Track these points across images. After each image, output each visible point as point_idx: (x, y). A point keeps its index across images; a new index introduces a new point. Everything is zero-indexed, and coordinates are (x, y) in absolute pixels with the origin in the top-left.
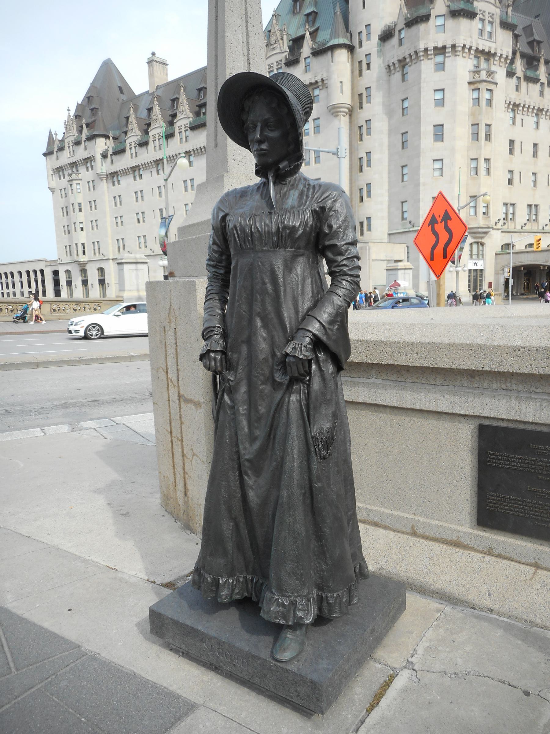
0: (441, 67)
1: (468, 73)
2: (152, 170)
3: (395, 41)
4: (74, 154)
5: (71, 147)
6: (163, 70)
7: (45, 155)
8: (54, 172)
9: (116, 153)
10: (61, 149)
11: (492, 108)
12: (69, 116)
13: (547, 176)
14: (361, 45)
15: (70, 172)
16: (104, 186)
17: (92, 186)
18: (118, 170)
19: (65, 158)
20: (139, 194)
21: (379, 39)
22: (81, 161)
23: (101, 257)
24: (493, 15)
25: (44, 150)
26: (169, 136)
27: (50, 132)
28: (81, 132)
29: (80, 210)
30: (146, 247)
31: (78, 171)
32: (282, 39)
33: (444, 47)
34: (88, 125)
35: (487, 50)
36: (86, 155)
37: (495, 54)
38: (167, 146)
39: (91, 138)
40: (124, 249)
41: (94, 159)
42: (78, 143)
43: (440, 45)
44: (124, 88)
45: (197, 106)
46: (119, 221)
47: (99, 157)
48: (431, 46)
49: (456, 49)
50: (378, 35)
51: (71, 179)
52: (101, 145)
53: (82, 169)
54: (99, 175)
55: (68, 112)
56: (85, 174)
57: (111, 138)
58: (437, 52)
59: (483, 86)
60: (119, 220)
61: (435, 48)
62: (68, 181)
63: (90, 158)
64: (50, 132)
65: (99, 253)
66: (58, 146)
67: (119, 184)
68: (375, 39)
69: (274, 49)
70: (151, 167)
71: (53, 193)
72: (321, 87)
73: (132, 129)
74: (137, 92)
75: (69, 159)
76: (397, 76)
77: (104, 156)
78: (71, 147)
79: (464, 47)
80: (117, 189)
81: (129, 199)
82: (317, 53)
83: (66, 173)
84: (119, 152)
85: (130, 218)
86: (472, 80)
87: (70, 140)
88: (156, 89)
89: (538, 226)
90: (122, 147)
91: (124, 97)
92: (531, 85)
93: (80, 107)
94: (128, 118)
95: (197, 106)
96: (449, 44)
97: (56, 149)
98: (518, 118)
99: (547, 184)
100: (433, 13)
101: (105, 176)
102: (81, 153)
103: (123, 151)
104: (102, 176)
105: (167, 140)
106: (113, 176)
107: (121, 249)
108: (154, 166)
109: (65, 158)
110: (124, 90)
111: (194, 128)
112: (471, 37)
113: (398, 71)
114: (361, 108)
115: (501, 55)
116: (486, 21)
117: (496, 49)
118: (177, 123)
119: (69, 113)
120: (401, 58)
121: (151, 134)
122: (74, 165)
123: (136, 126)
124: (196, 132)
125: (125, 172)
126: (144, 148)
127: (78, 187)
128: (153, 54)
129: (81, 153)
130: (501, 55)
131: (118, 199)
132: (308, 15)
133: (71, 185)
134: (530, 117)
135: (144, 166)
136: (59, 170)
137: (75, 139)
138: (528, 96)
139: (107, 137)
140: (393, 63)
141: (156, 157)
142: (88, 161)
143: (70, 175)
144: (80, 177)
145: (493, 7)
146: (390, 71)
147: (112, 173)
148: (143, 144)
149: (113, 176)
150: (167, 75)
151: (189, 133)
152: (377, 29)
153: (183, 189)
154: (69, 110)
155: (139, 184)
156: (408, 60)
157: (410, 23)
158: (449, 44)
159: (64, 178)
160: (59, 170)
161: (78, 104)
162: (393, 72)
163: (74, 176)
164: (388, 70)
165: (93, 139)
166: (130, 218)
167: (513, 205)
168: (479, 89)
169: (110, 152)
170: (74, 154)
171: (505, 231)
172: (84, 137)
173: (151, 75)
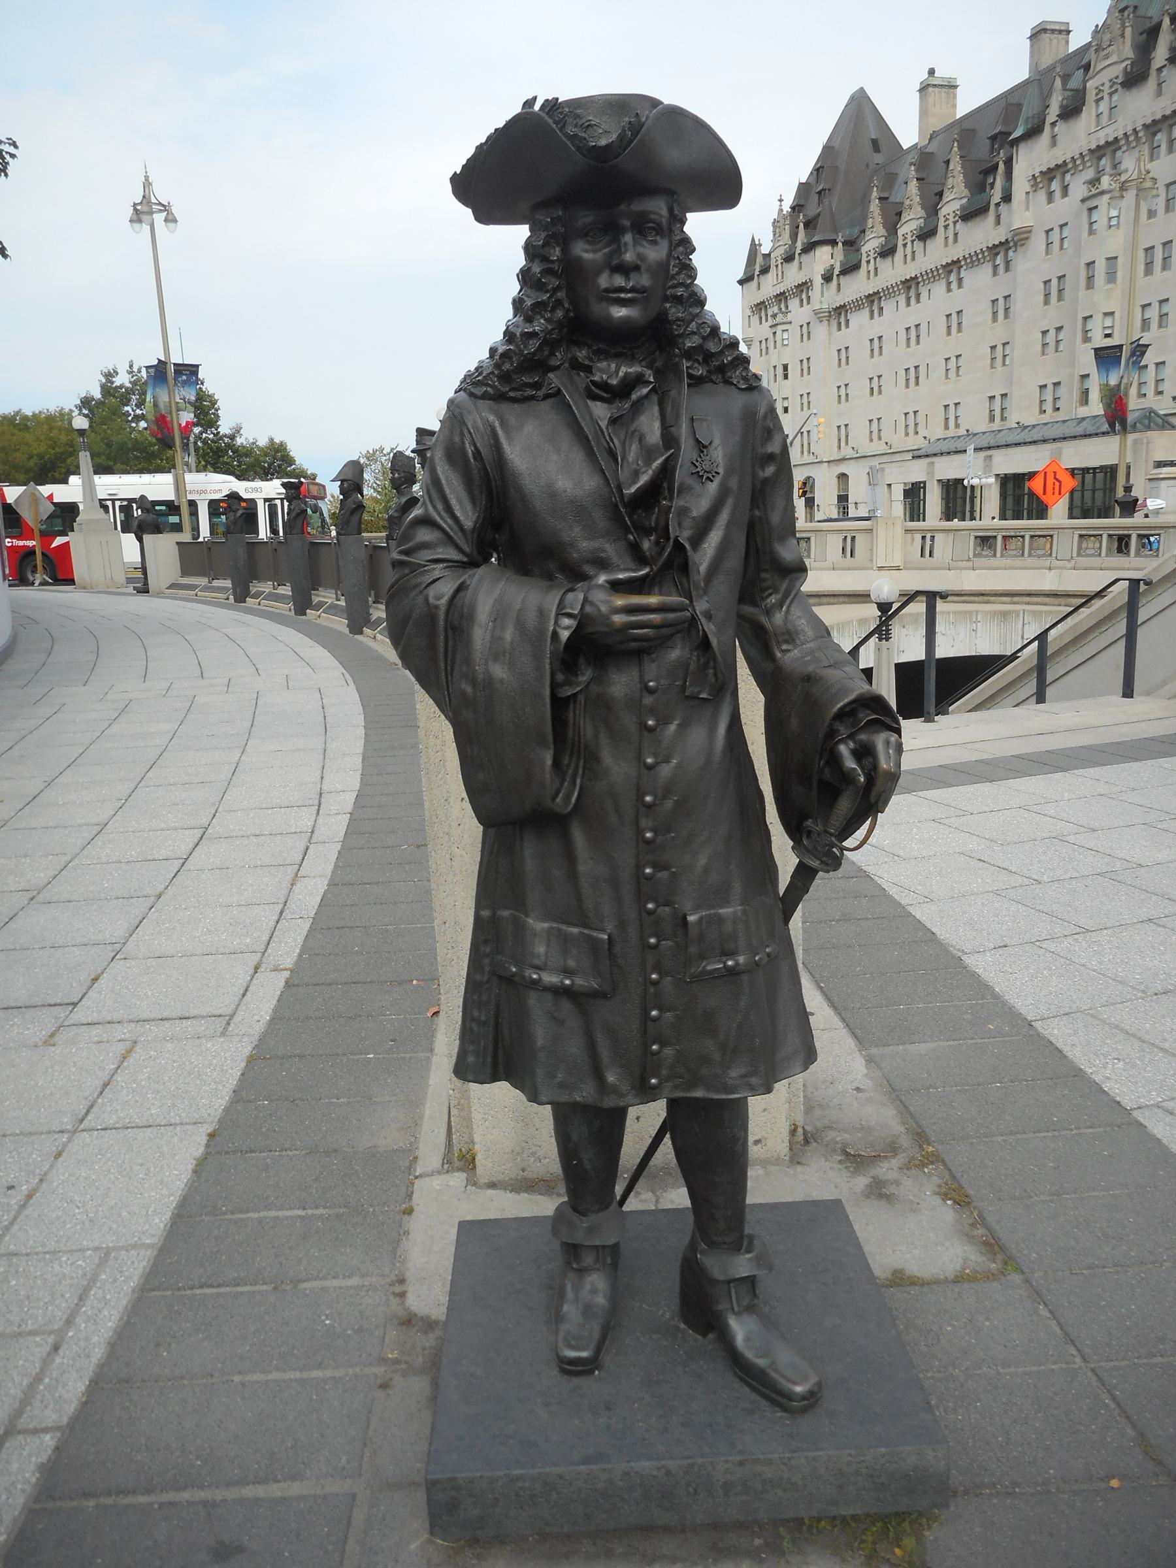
2: (898, 298)
4: (783, 278)
5: (780, 266)
7: (741, 282)
8: (753, 312)
9: (845, 272)
10: (765, 271)
12: (781, 210)
15: (776, 309)
16: (821, 331)
17: (806, 332)
19: (769, 286)
20: (876, 345)
22: (792, 290)
23: (812, 459)
25: (740, 275)
26: (926, 235)
27: (753, 238)
29: (786, 377)
30: (880, 438)
31: (787, 307)
32: (1123, 36)
34: (807, 225)
38: (923, 253)
39: (809, 248)
40: (847, 443)
41: (812, 285)
42: (789, 259)
45: (980, 173)
46: (843, 395)
47: (818, 280)
51: (775, 322)
52: (824, 258)
53: (794, 304)
54: (816, 314)
55: (779, 203)
56: (798, 312)
57: (840, 244)
60: (843, 392)
62: (770, 327)
63: (806, 283)
64: (753, 240)
66: (761, 266)
67: (847, 326)
69: (1107, 57)
73: (872, 227)
74: (906, 145)
75: (774, 288)
77: (827, 278)
78: (780, 266)
80: (843, 337)
81: (859, 353)
83: (770, 313)
84: (850, 269)
85: (859, 388)
87: (781, 251)
88: (930, 140)
90: (855, 262)
91: (879, 158)
93: (803, 189)
94: (948, 162)
97: (757, 273)
102: (793, 275)
103: (856, 267)
104: (822, 315)
105: (925, 241)
106: (840, 312)
107: (843, 444)
109: (769, 286)
110: (882, 144)
111: (970, 214)
118: (943, 209)
119: (781, 206)
122: (781, 297)
123: (879, 219)
125: (857, 305)
127: (785, 336)
128: (932, 72)
129: (793, 275)
131: (843, 355)
133: (775, 333)
135: (935, 273)
136: (761, 306)
137: (786, 251)
139: (833, 243)
141: (905, 274)
142: (803, 287)
143: (774, 316)
144: (790, 317)
147: (837, 308)
148: (887, 252)
150: (954, 106)
151: (959, 225)
153: (944, 329)
154: (781, 200)
155: (877, 326)
159: (767, 320)
161: (801, 184)
163: (780, 318)
165: (811, 249)
166: (859, 388)
169: (836, 272)
170: (783, 278)
172: (799, 246)
173: (924, 113)
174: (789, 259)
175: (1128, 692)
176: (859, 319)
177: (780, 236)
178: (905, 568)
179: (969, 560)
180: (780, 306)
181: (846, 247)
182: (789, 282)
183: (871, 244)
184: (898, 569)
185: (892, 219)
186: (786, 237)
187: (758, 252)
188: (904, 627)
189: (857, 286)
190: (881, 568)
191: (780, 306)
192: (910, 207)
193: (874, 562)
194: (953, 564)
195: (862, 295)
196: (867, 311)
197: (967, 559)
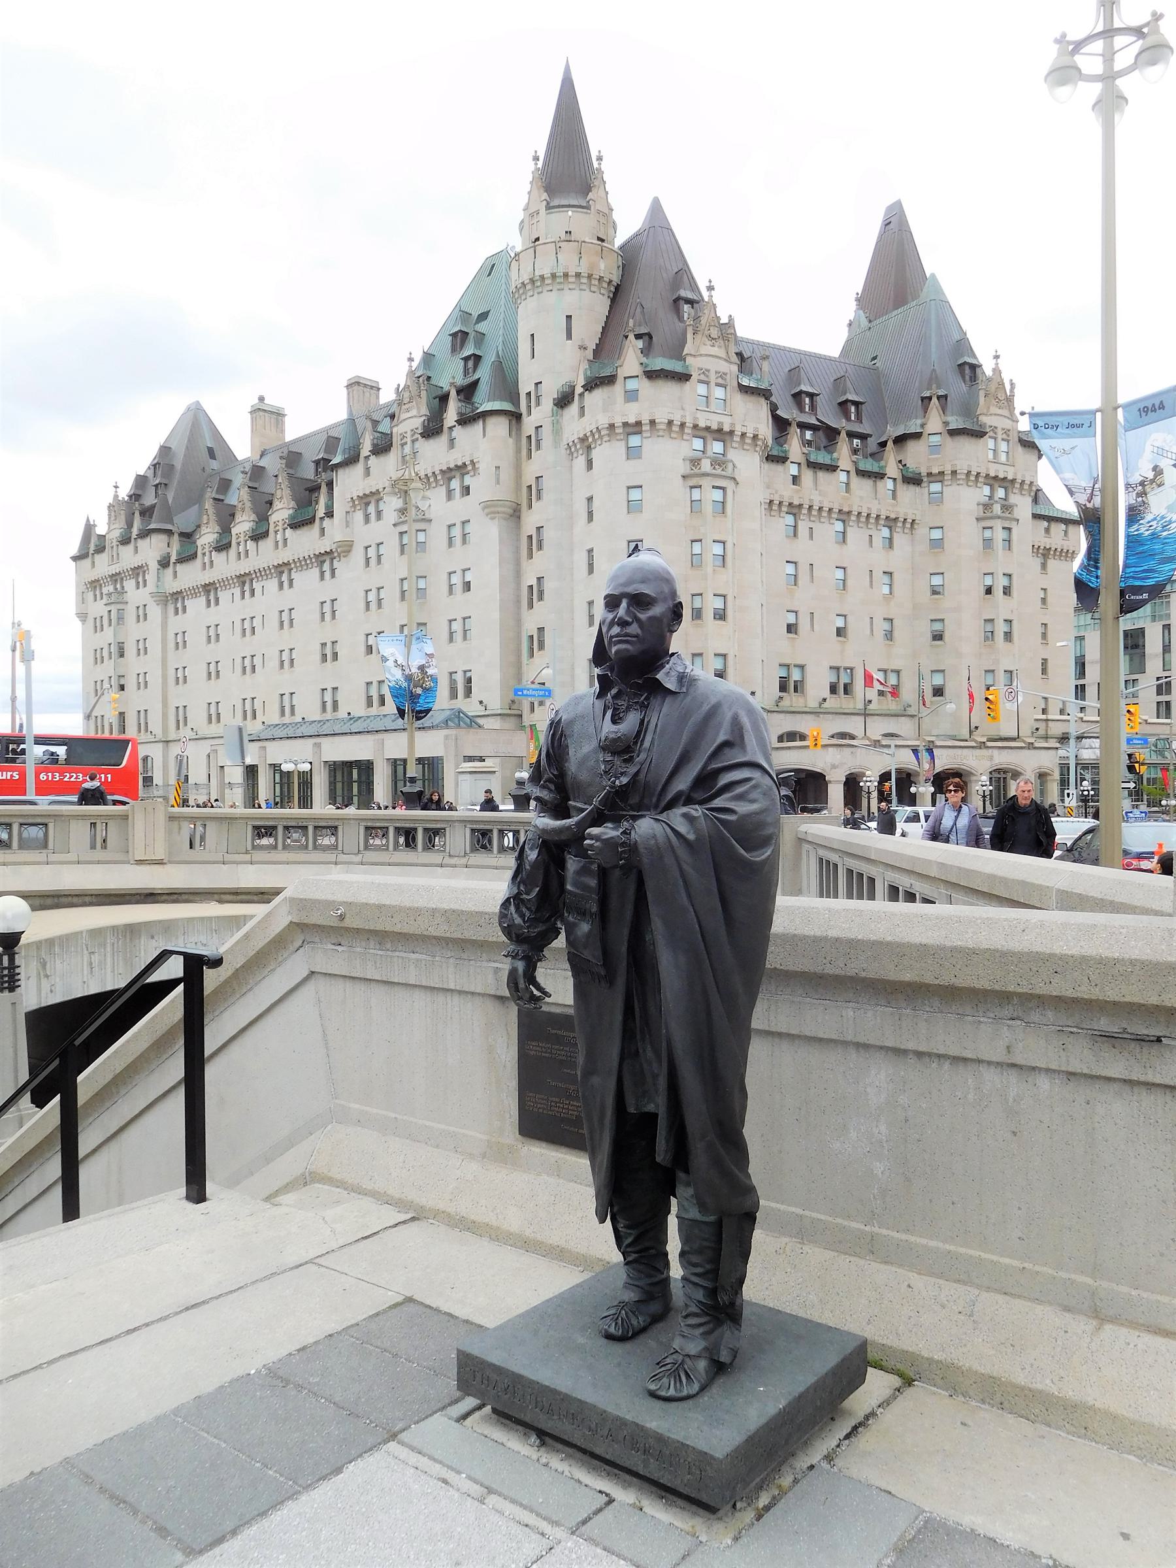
0: (633, 453)
1: (682, 461)
2: (233, 591)
3: (574, 408)
4: (118, 559)
5: (115, 548)
6: (277, 424)
7: (75, 559)
9: (181, 561)
11: (726, 517)
12: (116, 496)
13: (869, 620)
14: (529, 413)
15: (111, 588)
17: (142, 615)
18: (183, 588)
19: (103, 566)
21: (554, 405)
23: (151, 738)
24: (725, 374)
25: (74, 550)
27: (88, 520)
28: (130, 525)
31: (123, 587)
32: (419, 396)
33: (639, 424)
34: (142, 514)
35: (715, 427)
36: (137, 561)
37: (731, 433)
38: (255, 553)
39: (145, 534)
43: (632, 420)
44: (217, 450)
45: (306, 490)
47: (153, 566)
48: (618, 421)
49: (658, 427)
50: (554, 399)
51: (110, 601)
53: (129, 584)
57: (176, 537)
58: (631, 430)
59: (706, 483)
61: (625, 424)
64: (88, 520)
65: (147, 730)
68: (547, 404)
69: (408, 411)
70: (224, 588)
71: (83, 624)
72: (472, 473)
76: (581, 461)
77: (164, 563)
78: (115, 548)
79: (670, 423)
82: (464, 421)
84: (187, 557)
85: (196, 673)
86: (688, 471)
87: (116, 534)
88: (261, 456)
89: (855, 703)
90: (193, 552)
91: (214, 465)
92: (821, 475)
93: (141, 481)
95: (306, 490)
96: (645, 420)
98: (803, 527)
99: (868, 632)
100: (622, 373)
101: (163, 599)
108: (237, 585)
112: (683, 409)
113: (582, 455)
114: (530, 506)
115: (743, 435)
116: (712, 384)
117: (733, 424)
118: (273, 516)
119: (116, 492)
120: (581, 436)
121: (234, 531)
122: (116, 578)
123: (213, 517)
124: (299, 532)
125: (193, 592)
126: (223, 555)
128: (261, 399)
129: (128, 558)
130: (743, 435)
132: (466, 359)
133: (110, 611)
134: (826, 525)
136: (96, 584)
137: (121, 533)
138: (817, 492)
139: (169, 533)
140: (573, 441)
141: (240, 571)
142: (138, 571)
145: (726, 364)
146: (571, 454)
147: (174, 594)
149: (175, 599)
150: (283, 431)
151: (289, 531)
152: (550, 392)
153: (277, 624)
154: (116, 487)
155: (213, 615)
156: (590, 440)
157: (592, 384)
158: (645, 420)
159: (102, 599)
160: (95, 585)
162: (575, 455)
164: (568, 452)
165: (147, 536)
166: (196, 673)
167: (802, 667)
168: (700, 486)
169: (173, 559)
171: (785, 709)
172: (135, 531)
174: (125, 541)
175: (196, 1188)
176: (196, 605)
177: (116, 519)
178: (170, 862)
179: (247, 852)
180: (115, 586)
181: (182, 539)
182: (125, 564)
183: (207, 537)
184: (160, 862)
185: (227, 518)
186: (121, 524)
187: (93, 533)
188: (153, 937)
189: (190, 575)
190: (140, 862)
191: (115, 586)
192: (243, 510)
193: (131, 853)
194: (228, 857)
195: (199, 583)
196: (203, 599)
197: (244, 851)
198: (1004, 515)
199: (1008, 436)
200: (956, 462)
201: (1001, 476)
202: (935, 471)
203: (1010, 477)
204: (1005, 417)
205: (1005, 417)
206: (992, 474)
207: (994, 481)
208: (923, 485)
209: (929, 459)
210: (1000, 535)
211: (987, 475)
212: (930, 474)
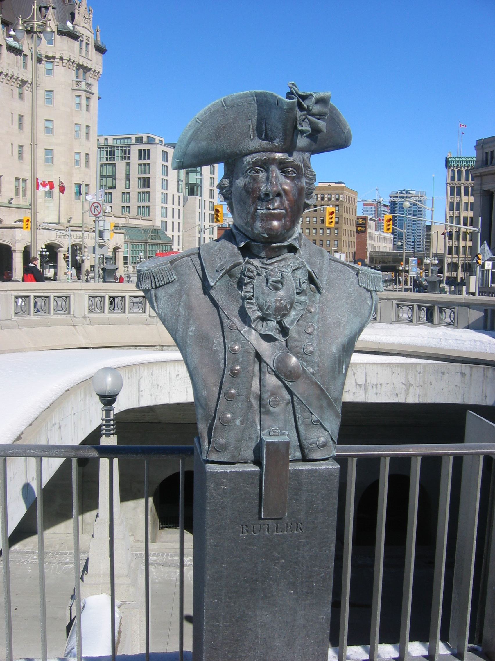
99: (10, 153)
198: (87, 89)
199: (88, 41)
200: (63, 52)
201: (85, 65)
202: (50, 55)
203: (89, 67)
204: (88, 29)
205: (88, 29)
206: (81, 63)
207: (80, 67)
208: (43, 62)
209: (46, 46)
210: (84, 101)
211: (79, 63)
212: (47, 57)
